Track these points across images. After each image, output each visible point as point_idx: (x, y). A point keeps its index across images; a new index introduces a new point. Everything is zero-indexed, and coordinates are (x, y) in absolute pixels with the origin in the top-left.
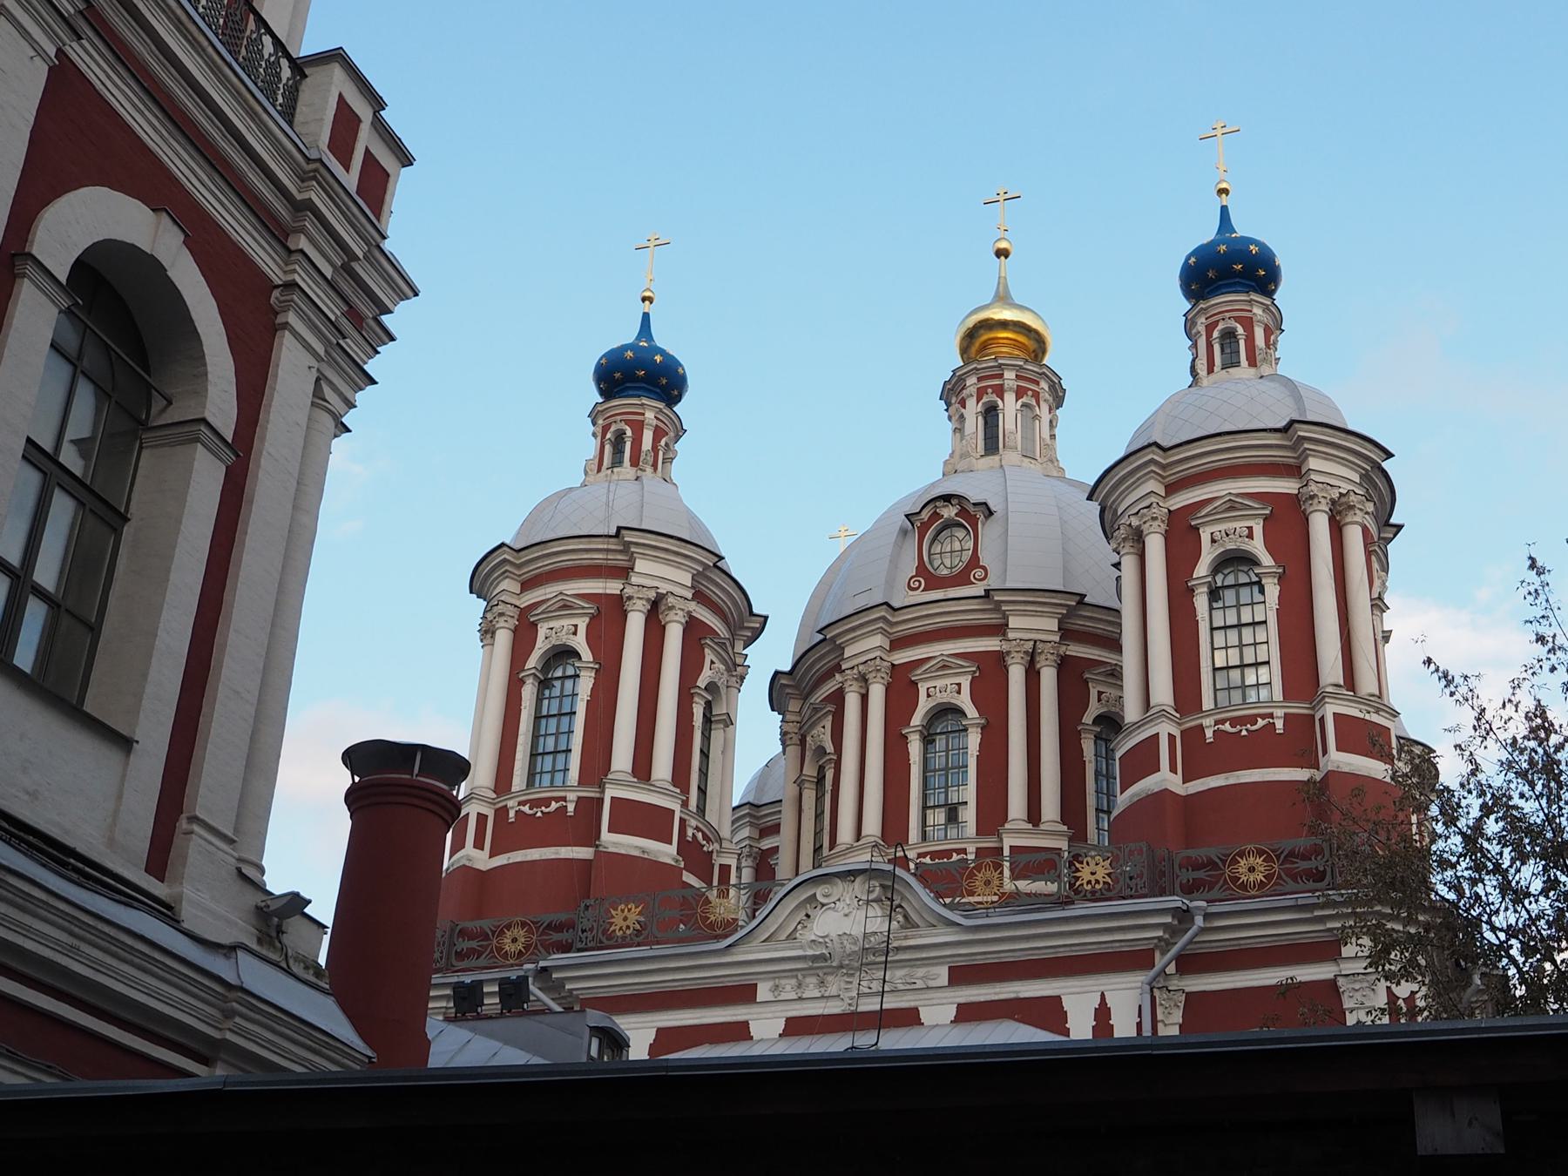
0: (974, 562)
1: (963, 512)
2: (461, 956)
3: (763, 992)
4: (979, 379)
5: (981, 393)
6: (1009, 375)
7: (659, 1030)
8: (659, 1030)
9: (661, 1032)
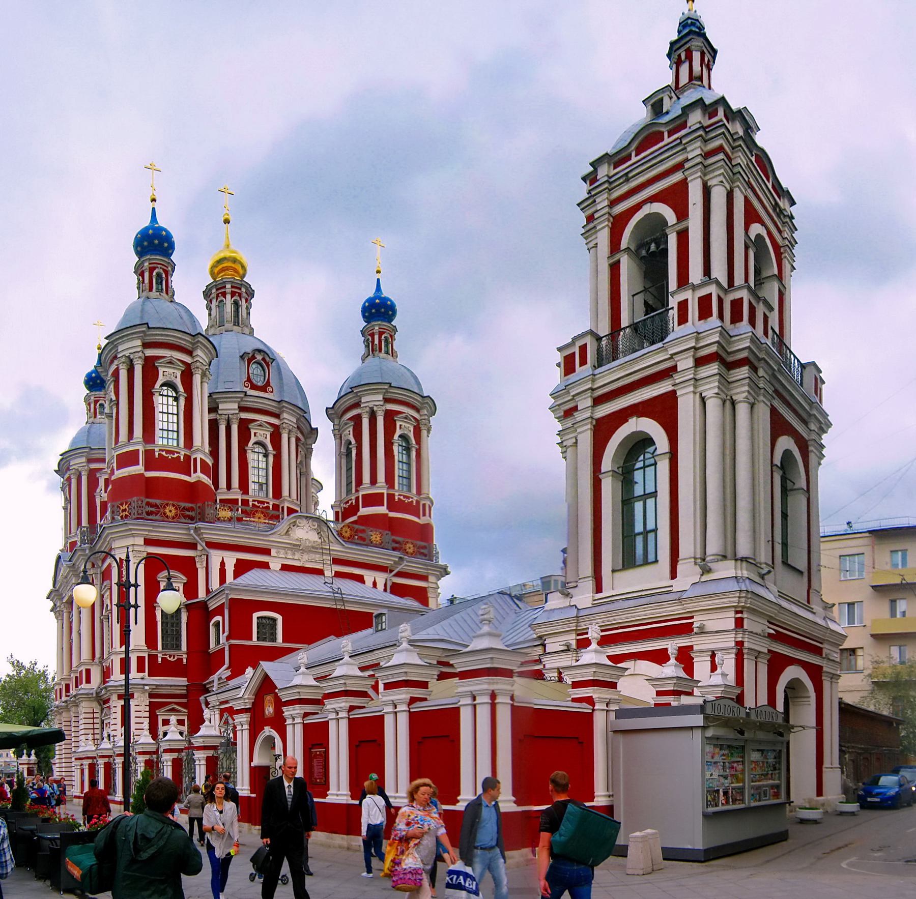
0: (268, 384)
1: (264, 359)
2: (148, 513)
3: (273, 552)
4: (232, 287)
5: (233, 294)
6: (229, 286)
7: (237, 560)
8: (237, 560)
9: (239, 561)
